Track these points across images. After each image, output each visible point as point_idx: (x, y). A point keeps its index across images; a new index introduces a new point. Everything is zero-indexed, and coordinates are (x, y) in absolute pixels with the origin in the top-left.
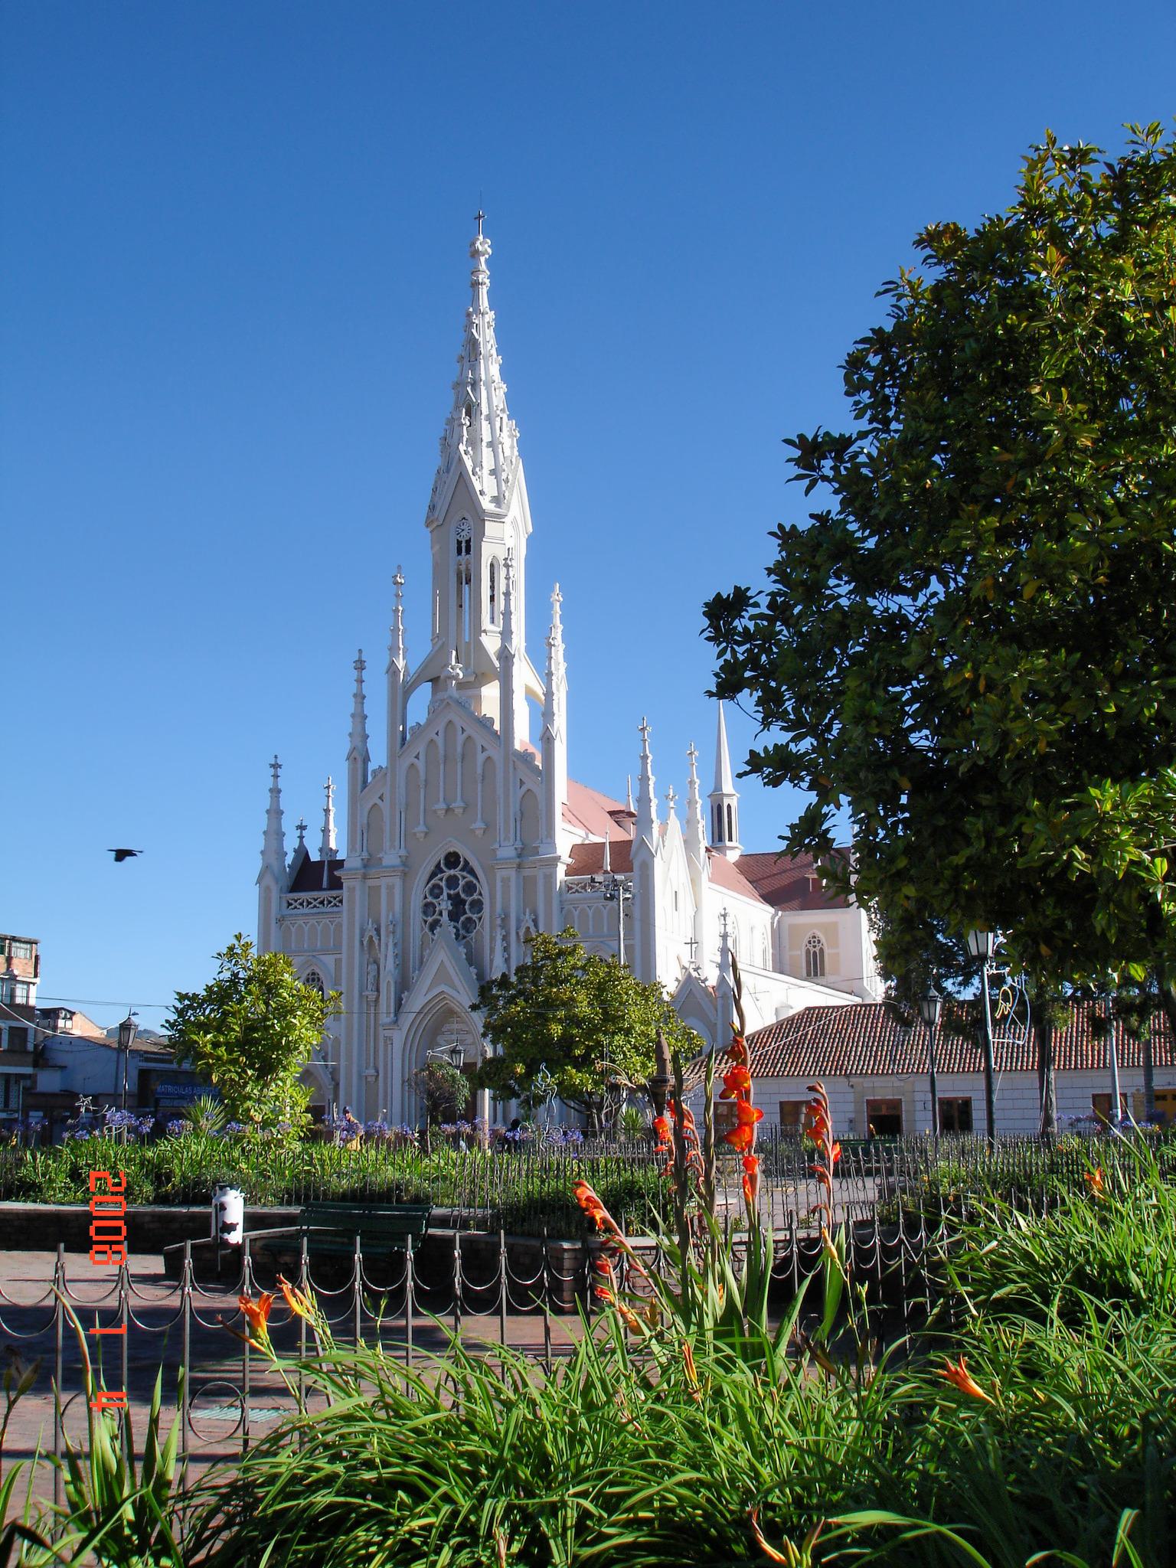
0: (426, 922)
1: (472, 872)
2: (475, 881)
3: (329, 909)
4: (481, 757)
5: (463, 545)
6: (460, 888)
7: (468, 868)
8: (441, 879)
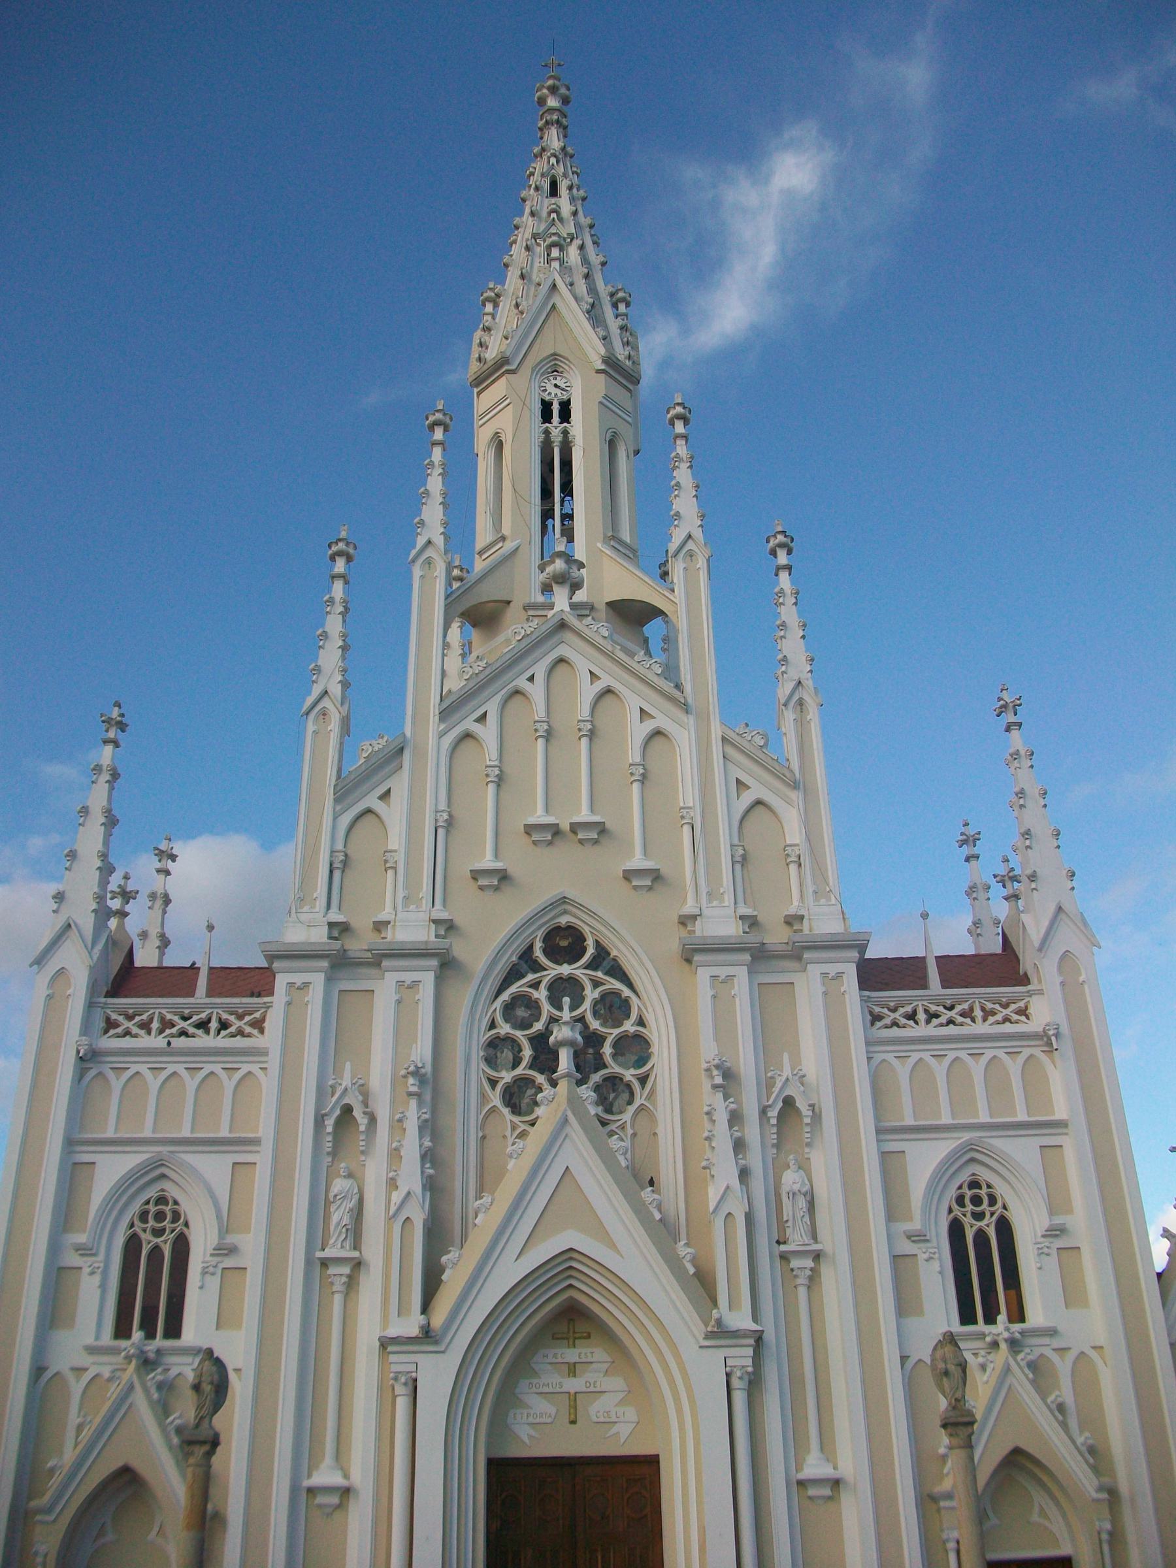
0: (493, 1083)
1: (618, 972)
2: (626, 992)
3: (222, 1041)
4: (639, 731)
5: (556, 408)
6: (587, 1005)
7: (602, 958)
8: (535, 985)
